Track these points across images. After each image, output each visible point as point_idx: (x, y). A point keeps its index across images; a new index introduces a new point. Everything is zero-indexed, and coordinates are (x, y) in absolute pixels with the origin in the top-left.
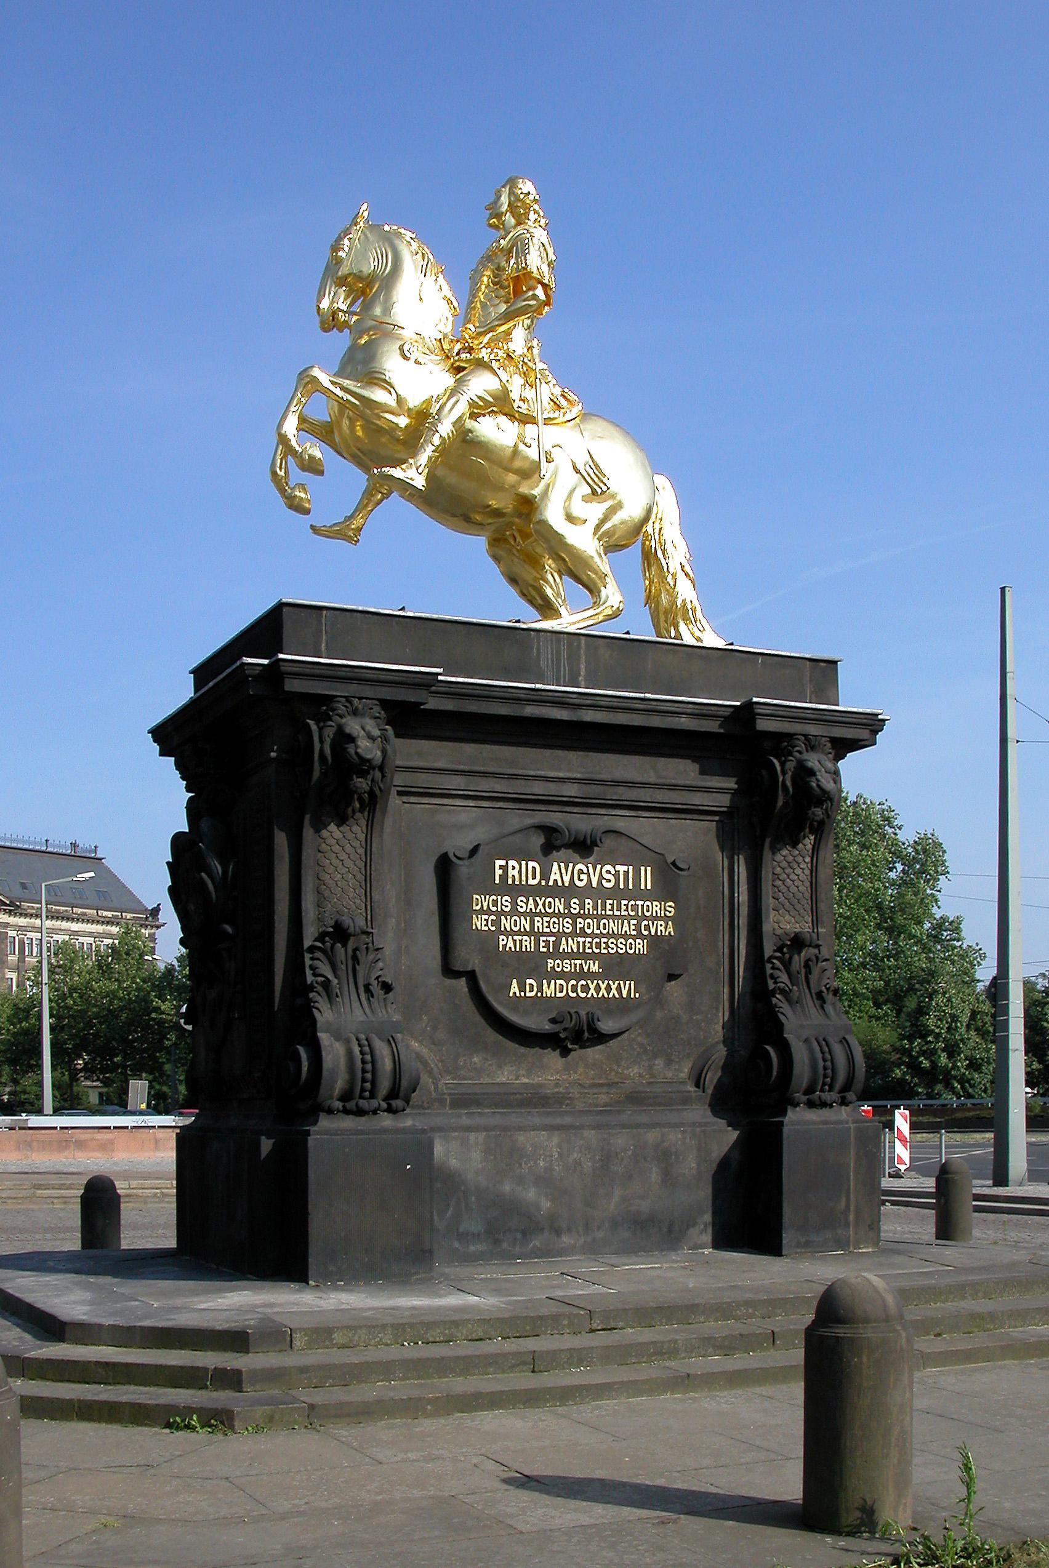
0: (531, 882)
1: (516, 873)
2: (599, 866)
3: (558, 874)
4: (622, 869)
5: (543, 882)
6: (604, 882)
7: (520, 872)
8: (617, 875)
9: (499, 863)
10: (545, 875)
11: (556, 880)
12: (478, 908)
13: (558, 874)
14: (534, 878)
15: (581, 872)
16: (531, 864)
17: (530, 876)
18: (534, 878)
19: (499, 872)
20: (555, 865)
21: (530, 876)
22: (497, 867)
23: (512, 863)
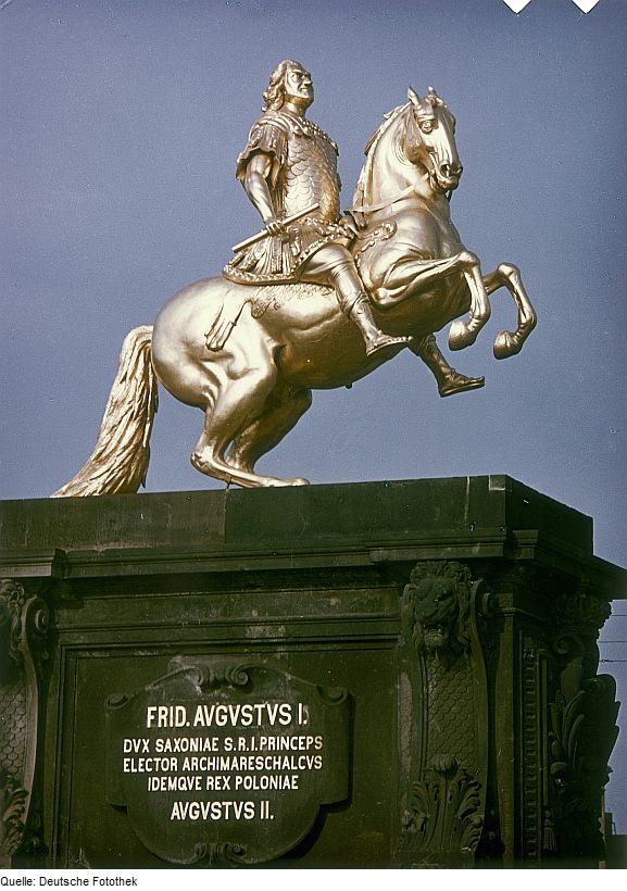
0: (177, 725)
1: (164, 717)
2: (239, 706)
3: (202, 717)
4: (260, 707)
5: (188, 724)
6: (243, 721)
7: (168, 717)
8: (255, 714)
9: (150, 709)
10: (190, 717)
11: (199, 723)
12: (129, 751)
13: (202, 717)
14: (180, 721)
15: (222, 712)
16: (178, 708)
17: (177, 719)
18: (180, 721)
19: (150, 717)
20: (200, 707)
21: (177, 719)
22: (149, 713)
23: (161, 709)
